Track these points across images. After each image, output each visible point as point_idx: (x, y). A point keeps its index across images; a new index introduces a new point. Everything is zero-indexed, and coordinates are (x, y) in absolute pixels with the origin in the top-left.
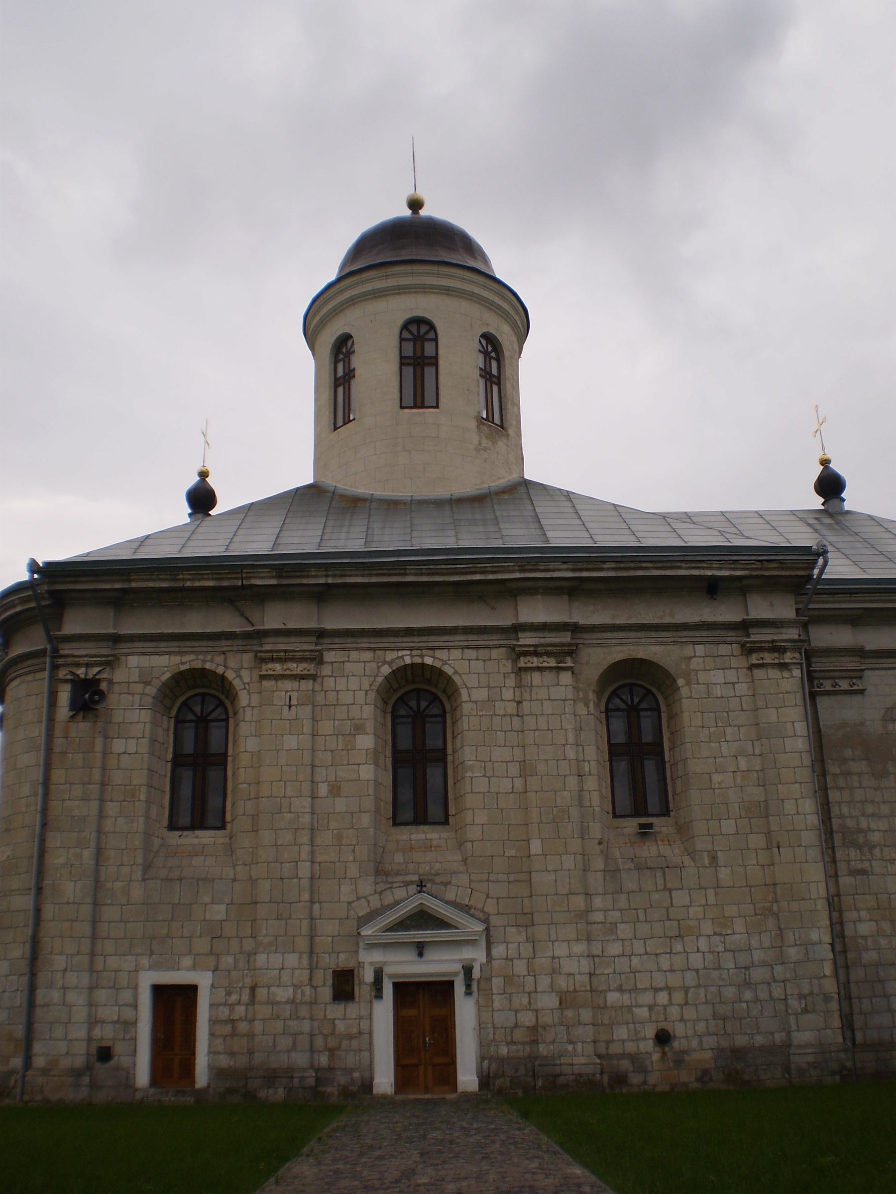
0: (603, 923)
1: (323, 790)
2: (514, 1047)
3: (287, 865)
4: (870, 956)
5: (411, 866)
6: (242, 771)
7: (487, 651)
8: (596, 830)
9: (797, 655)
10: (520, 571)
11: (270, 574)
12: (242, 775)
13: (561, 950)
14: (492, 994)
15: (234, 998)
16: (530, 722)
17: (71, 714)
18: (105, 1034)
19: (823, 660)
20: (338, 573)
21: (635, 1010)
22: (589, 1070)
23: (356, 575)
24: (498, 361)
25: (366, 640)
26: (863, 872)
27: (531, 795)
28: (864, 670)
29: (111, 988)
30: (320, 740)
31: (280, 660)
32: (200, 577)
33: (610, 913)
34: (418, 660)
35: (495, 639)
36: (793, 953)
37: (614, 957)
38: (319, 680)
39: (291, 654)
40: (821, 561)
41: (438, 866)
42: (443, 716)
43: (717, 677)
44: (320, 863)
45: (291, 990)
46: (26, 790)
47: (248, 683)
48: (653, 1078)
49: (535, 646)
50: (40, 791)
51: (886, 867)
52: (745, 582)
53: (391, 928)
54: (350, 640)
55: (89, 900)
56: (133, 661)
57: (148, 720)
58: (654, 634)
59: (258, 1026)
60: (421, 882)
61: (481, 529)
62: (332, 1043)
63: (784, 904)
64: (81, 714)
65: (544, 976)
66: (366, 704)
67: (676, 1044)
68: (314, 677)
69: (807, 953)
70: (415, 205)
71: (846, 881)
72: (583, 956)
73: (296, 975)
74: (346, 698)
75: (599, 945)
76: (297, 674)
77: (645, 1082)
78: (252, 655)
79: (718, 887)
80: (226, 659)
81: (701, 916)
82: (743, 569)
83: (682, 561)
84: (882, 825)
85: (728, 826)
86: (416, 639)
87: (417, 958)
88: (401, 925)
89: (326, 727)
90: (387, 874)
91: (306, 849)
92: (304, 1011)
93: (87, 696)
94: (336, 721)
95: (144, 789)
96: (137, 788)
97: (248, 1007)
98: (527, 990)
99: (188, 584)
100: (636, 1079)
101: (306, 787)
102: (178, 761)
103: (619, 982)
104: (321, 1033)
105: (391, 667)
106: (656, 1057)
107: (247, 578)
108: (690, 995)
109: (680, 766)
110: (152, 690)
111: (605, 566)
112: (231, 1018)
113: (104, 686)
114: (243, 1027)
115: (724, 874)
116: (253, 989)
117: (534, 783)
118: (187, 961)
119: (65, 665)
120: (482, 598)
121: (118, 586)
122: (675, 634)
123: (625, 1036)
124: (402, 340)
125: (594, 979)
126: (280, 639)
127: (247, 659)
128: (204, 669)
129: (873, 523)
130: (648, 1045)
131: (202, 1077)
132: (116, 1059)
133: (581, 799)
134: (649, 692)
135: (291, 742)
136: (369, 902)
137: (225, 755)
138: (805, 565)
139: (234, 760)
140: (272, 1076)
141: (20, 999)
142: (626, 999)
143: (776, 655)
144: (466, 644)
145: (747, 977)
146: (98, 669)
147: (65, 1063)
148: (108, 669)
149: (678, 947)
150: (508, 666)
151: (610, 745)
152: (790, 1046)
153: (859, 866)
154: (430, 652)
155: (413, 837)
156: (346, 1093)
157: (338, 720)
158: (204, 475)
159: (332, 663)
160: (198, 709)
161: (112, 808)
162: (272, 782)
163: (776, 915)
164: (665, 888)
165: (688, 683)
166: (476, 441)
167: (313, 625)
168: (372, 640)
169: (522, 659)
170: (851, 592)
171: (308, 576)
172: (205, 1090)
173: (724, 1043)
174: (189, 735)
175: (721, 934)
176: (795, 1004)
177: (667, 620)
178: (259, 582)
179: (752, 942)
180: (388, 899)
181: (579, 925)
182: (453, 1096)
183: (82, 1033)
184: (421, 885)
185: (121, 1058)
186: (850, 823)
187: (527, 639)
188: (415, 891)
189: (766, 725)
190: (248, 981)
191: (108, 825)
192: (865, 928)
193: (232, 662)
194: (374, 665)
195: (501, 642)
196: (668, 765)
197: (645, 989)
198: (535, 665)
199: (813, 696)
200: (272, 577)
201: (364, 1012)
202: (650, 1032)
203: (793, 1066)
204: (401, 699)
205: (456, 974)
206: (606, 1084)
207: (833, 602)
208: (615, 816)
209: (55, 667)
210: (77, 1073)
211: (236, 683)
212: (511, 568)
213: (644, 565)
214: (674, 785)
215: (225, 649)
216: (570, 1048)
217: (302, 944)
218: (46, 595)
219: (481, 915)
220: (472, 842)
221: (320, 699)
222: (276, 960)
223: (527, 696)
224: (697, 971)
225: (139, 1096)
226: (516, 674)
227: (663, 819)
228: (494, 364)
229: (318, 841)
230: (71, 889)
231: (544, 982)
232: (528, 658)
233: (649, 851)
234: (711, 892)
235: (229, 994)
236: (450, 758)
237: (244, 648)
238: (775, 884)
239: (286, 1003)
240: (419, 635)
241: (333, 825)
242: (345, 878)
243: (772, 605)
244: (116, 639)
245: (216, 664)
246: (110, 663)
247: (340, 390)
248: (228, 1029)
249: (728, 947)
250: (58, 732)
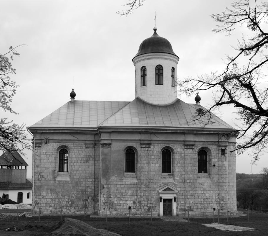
70: (155, 30)
124: (156, 69)
247: (142, 78)
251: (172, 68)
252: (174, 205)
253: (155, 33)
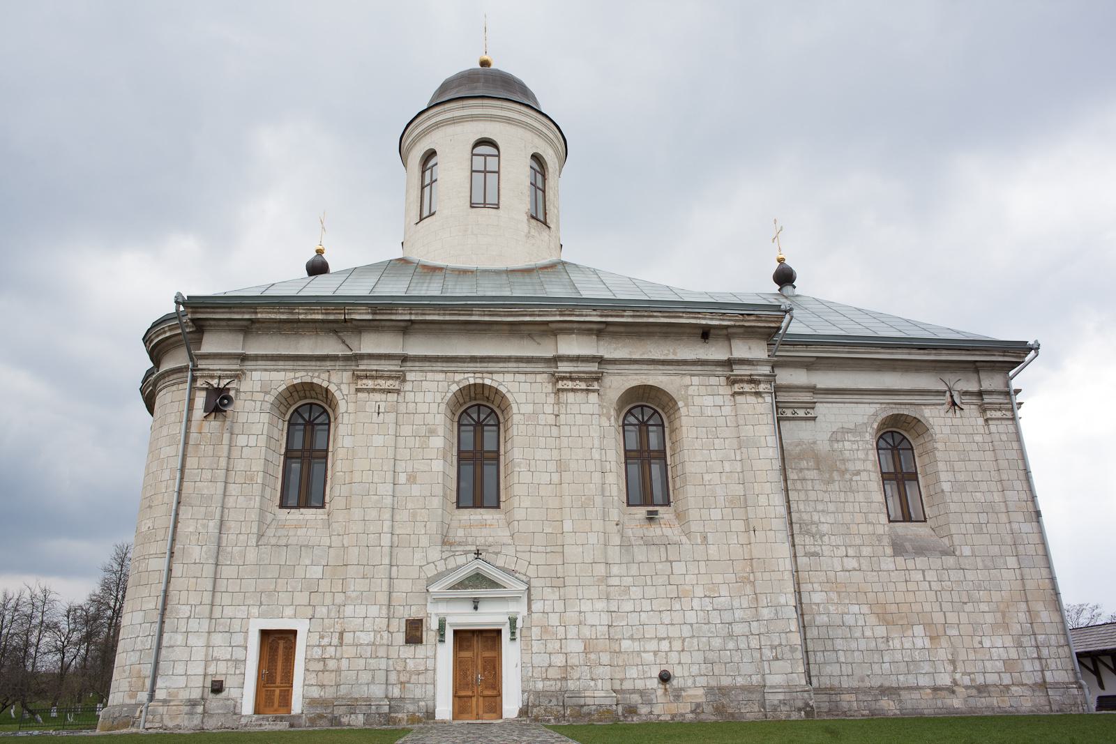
0: (618, 586)
1: (402, 478)
2: (548, 683)
3: (373, 536)
4: (822, 619)
5: (470, 540)
6: (339, 462)
7: (533, 376)
8: (614, 515)
9: (769, 386)
10: (561, 315)
11: (367, 311)
12: (339, 465)
13: (586, 606)
14: (532, 640)
15: (325, 641)
16: (565, 430)
17: (205, 414)
18: (219, 670)
19: (784, 394)
20: (420, 312)
21: (642, 654)
22: (608, 701)
23: (434, 314)
24: (544, 176)
25: (439, 364)
26: (815, 554)
27: (565, 486)
28: (816, 402)
29: (226, 632)
30: (401, 440)
31: (372, 377)
32: (311, 312)
33: (625, 578)
34: (479, 381)
35: (540, 367)
36: (766, 613)
37: (628, 612)
38: (402, 394)
39: (381, 373)
40: (788, 316)
41: (491, 539)
42: (498, 425)
43: (708, 401)
44: (398, 535)
45: (372, 634)
46: (166, 475)
47: (347, 395)
48: (657, 710)
49: (570, 372)
50: (178, 476)
51: (833, 550)
52: (730, 330)
53: (453, 588)
54: (427, 364)
55: (212, 561)
56: (256, 375)
57: (266, 421)
58: (661, 367)
59: (344, 663)
60: (478, 551)
61: (530, 287)
62: (403, 679)
63: (758, 575)
64: (213, 414)
65: (571, 627)
66: (438, 413)
67: (674, 682)
68: (398, 392)
69: (777, 613)
71: (802, 561)
72: (603, 611)
73: (376, 623)
74: (423, 408)
75: (615, 603)
76: (385, 389)
77: (651, 713)
78: (351, 373)
79: (708, 560)
80: (329, 375)
81: (695, 582)
82: (729, 320)
83: (683, 312)
84: (830, 519)
85: (716, 514)
86: (478, 365)
87: (474, 611)
88: (461, 585)
89: (406, 430)
90: (451, 545)
91: (387, 524)
92: (382, 652)
93: (218, 401)
94: (414, 426)
95: (261, 474)
96: (256, 473)
97: (338, 648)
98: (559, 637)
99: (301, 317)
100: (644, 710)
101: (389, 476)
102: (289, 455)
103: (630, 633)
104: (395, 669)
105: (458, 385)
106: (660, 692)
107: (348, 314)
108: (686, 644)
109: (679, 467)
110: (270, 399)
111: (626, 314)
112: (323, 657)
113: (232, 393)
114: (332, 664)
115: (713, 550)
116: (341, 634)
117: (567, 476)
118: (289, 611)
119: (201, 377)
120: (530, 336)
121: (247, 316)
122: (677, 367)
123: (635, 676)
125: (612, 630)
126: (373, 362)
127: (347, 376)
128: (312, 383)
129: (817, 303)
130: (654, 683)
131: (297, 706)
132: (227, 689)
133: (603, 490)
134: (656, 411)
135: (378, 440)
136: (436, 566)
137: (327, 451)
138: (776, 319)
139: (333, 454)
140: (352, 707)
141: (151, 643)
142: (636, 646)
143: (753, 385)
144: (517, 370)
145: (730, 630)
146: (228, 381)
147: (184, 695)
148: (236, 381)
149: (677, 606)
150: (549, 388)
151: (626, 451)
152: (765, 686)
153: (813, 549)
154: (490, 376)
155: (472, 517)
156: (413, 719)
157: (416, 425)
158: (320, 252)
159: (413, 381)
160: (306, 416)
161: (233, 489)
162: (362, 471)
163: (753, 583)
164: (667, 561)
165: (687, 405)
166: (526, 230)
167: (398, 350)
168: (444, 365)
169: (560, 382)
170: (807, 344)
171: (396, 314)
172: (299, 716)
173: (713, 683)
175: (709, 597)
176: (768, 653)
177: (671, 357)
178: (357, 317)
179: (734, 603)
180: (451, 564)
181: (600, 587)
182: (500, 721)
183: (200, 671)
184: (478, 553)
185: (230, 692)
186: (805, 517)
187: (564, 367)
188: (473, 558)
189: (745, 438)
190: (338, 628)
191: (230, 502)
192: (818, 598)
193: (335, 377)
194: (446, 384)
195: (545, 370)
196: (669, 467)
197: (651, 638)
198: (570, 387)
199: (779, 420)
200: (369, 313)
201: (430, 654)
202: (656, 673)
203: (767, 701)
204: (465, 411)
205: (504, 624)
206: (620, 714)
207: (793, 351)
208: (628, 505)
209: (194, 379)
210: (193, 704)
211: (337, 395)
212: (554, 313)
213: (655, 314)
214: (674, 482)
215: (329, 368)
216: (592, 683)
217: (382, 598)
218: (190, 324)
219: (524, 578)
220: (518, 521)
221: (402, 408)
222: (361, 611)
223: (563, 411)
224: (691, 625)
225: (243, 721)
226: (555, 394)
227: (665, 508)
228: (539, 177)
229: (397, 518)
230: (196, 553)
231: (573, 632)
232: (565, 382)
233: (655, 531)
234: (702, 564)
235: (322, 637)
236: (502, 458)
237: (344, 368)
238: (752, 559)
239: (368, 645)
240: (481, 362)
241: (409, 506)
242: (418, 547)
243: (750, 348)
244: (244, 358)
245: (320, 379)
246: (237, 376)
248: (320, 666)
249: (715, 607)
250: (193, 429)
251: (528, 161)
252: (511, 653)
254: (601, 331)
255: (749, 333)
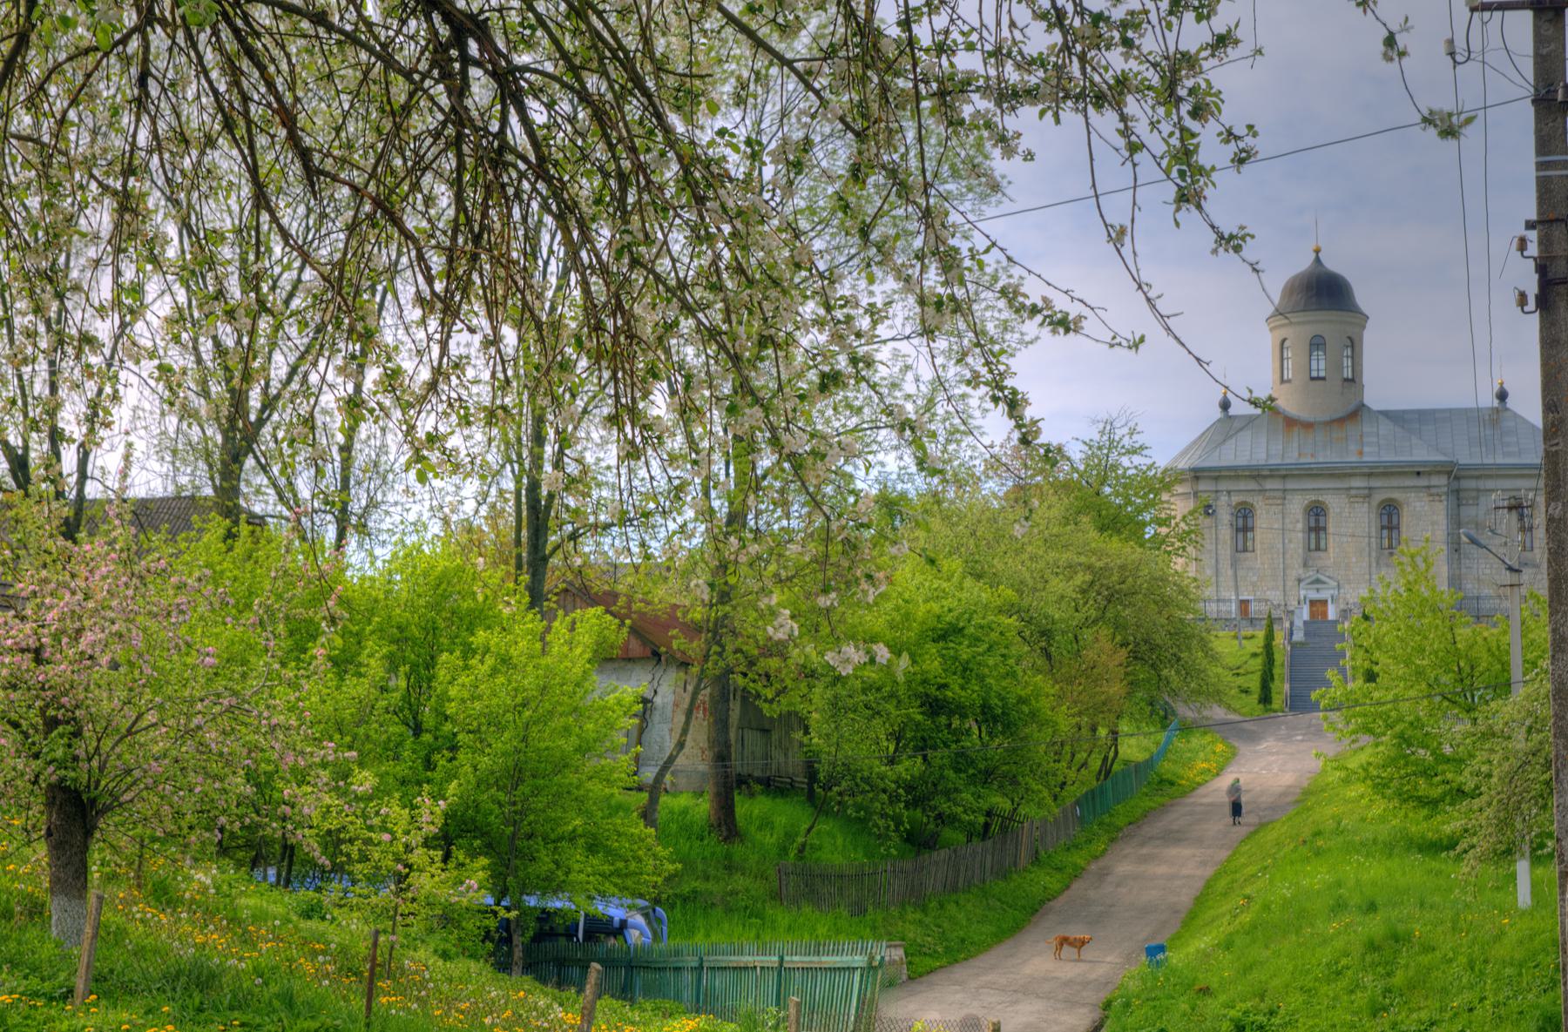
70: (1317, 251)
174: (1241, 522)
245: (1249, 500)
246: (1217, 499)
253: (1318, 260)
254: (1370, 475)
255: (1439, 473)
